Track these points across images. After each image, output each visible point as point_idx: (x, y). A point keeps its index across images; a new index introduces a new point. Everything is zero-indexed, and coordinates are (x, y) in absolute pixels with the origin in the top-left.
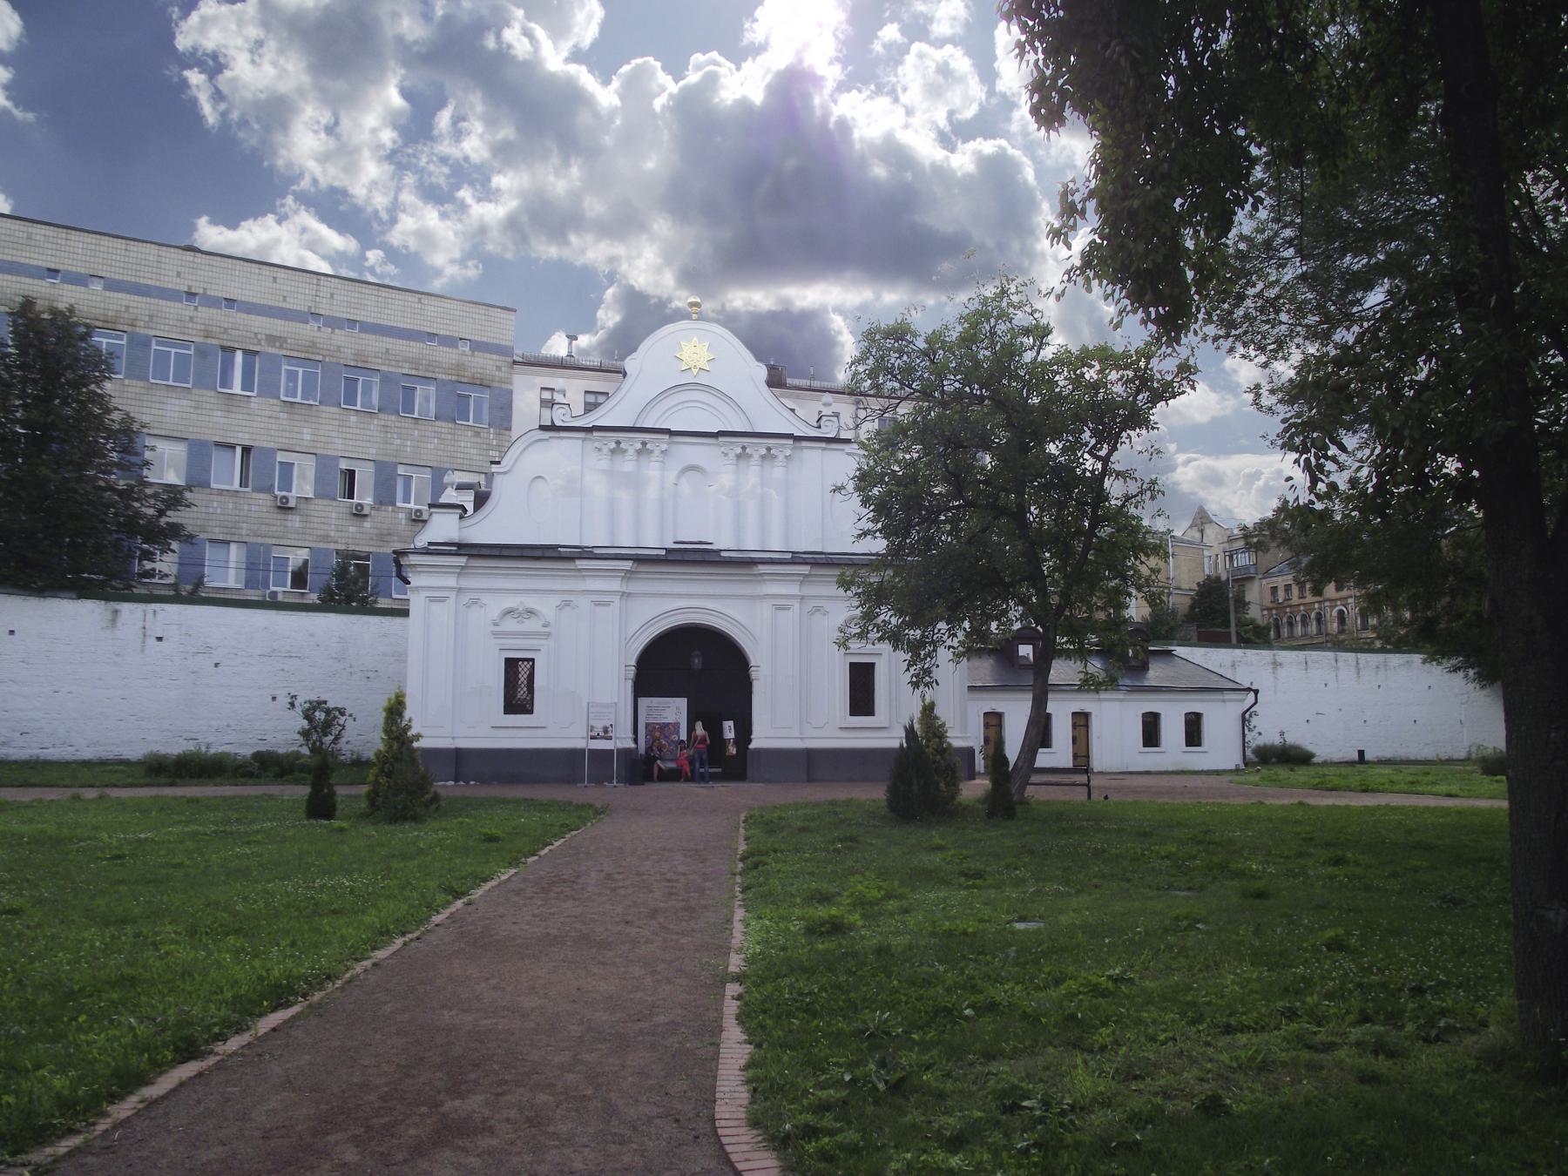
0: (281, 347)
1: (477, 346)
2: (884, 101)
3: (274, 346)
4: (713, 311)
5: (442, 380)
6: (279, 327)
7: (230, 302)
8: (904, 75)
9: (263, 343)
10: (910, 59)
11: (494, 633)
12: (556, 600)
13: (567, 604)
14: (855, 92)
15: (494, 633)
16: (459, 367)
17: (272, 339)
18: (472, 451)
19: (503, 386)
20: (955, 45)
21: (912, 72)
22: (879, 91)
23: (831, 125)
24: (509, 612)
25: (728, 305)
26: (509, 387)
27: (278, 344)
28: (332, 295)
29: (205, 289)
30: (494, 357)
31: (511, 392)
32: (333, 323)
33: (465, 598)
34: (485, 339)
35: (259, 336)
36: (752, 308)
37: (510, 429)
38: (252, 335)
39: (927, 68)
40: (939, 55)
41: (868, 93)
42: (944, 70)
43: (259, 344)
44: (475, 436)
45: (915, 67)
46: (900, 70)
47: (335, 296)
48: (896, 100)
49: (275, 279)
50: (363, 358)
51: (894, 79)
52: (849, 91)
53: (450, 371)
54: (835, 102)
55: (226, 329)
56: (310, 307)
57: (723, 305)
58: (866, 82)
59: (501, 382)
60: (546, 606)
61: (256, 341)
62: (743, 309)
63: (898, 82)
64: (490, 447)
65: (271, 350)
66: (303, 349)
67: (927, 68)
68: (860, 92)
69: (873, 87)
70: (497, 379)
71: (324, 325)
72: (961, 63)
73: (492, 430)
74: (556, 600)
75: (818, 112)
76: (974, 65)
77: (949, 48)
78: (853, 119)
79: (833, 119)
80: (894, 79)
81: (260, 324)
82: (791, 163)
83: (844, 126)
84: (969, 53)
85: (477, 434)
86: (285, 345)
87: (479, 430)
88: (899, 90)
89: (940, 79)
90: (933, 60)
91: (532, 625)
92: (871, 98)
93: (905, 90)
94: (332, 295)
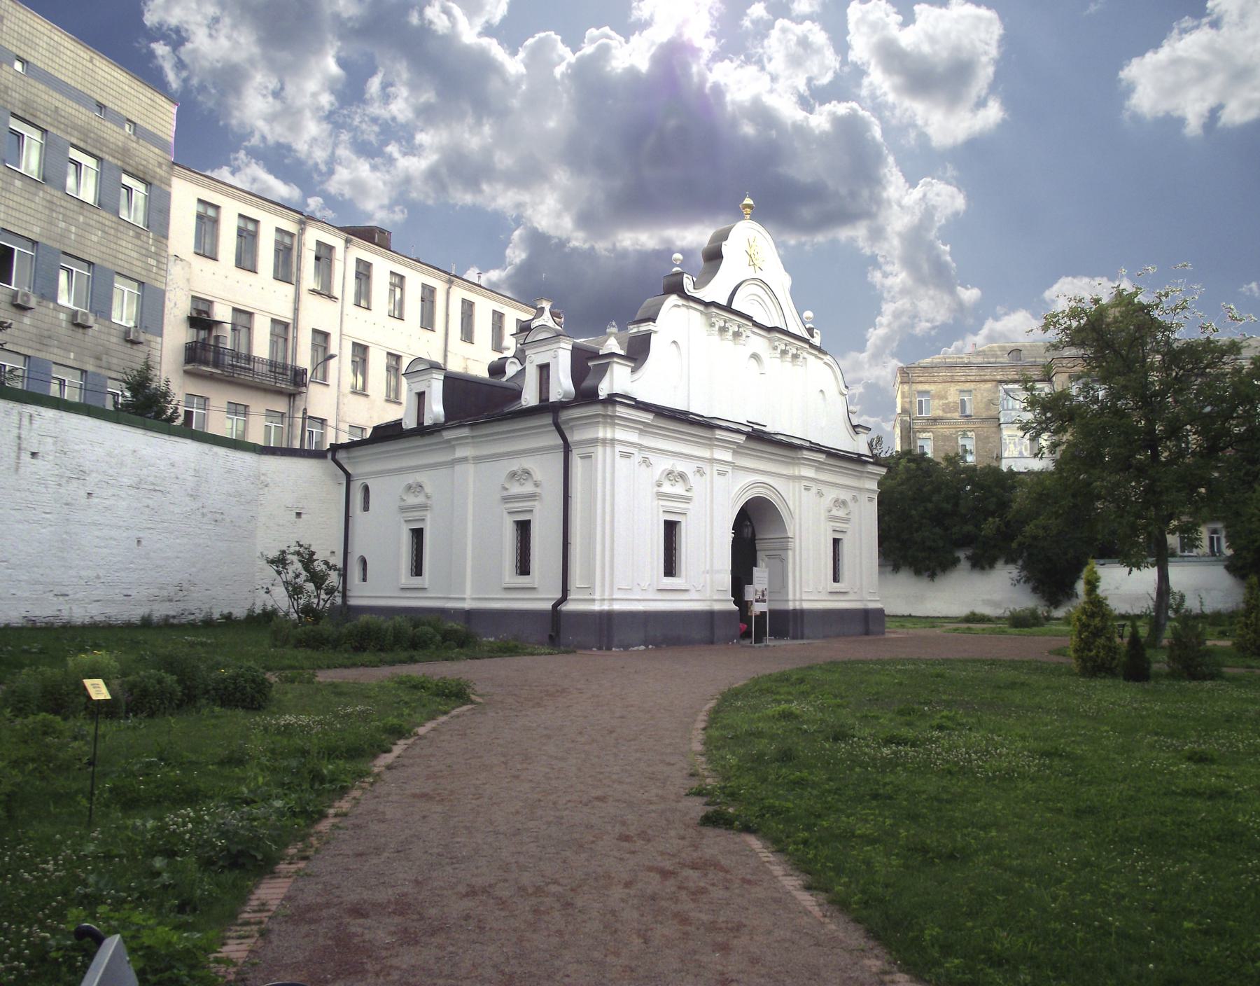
2: (752, 69)
4: (606, 250)
5: (109, 163)
8: (770, 47)
10: (775, 33)
14: (727, 61)
20: (813, 21)
21: (776, 45)
22: (748, 60)
23: (707, 90)
25: (618, 245)
36: (638, 247)
39: (789, 41)
40: (799, 29)
41: (739, 62)
42: (804, 43)
45: (780, 41)
46: (766, 42)
48: (763, 68)
51: (761, 51)
52: (722, 60)
53: (116, 154)
54: (710, 70)
57: (614, 245)
58: (737, 54)
62: (631, 248)
63: (764, 53)
67: (789, 41)
68: (732, 62)
69: (742, 57)
72: (819, 36)
75: (696, 79)
76: (830, 39)
77: (808, 24)
78: (725, 84)
79: (708, 85)
80: (761, 51)
82: (672, 123)
83: (718, 91)
84: (825, 28)
88: (765, 60)
89: (800, 51)
90: (794, 34)
92: (742, 67)
93: (770, 60)
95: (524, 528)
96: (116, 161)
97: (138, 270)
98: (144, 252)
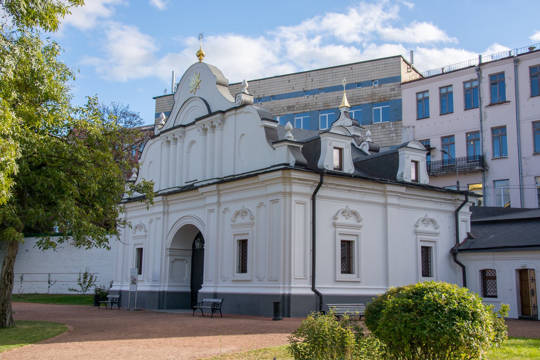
0: (293, 110)
1: (382, 82)
3: (290, 111)
6: (291, 101)
7: (273, 97)
9: (286, 110)
11: (232, 226)
12: (257, 202)
13: (261, 204)
15: (232, 226)
16: (373, 94)
17: (289, 108)
18: (381, 136)
19: (396, 98)
24: (237, 214)
26: (400, 98)
27: (291, 109)
28: (312, 80)
29: (264, 95)
30: (391, 84)
31: (400, 100)
32: (313, 92)
33: (222, 209)
34: (386, 77)
35: (284, 108)
37: (401, 120)
38: (282, 108)
43: (284, 111)
44: (382, 128)
47: (314, 80)
49: (289, 81)
50: (327, 105)
55: (272, 109)
56: (303, 89)
59: (395, 96)
60: (251, 206)
61: (283, 110)
64: (391, 132)
65: (289, 113)
66: (302, 108)
70: (393, 95)
71: (310, 95)
73: (391, 123)
74: (257, 202)
81: (285, 103)
85: (384, 127)
86: (294, 109)
87: (384, 125)
91: (247, 219)
94: (312, 80)
95: (426, 252)
96: (368, 101)
97: (386, 142)
98: (388, 132)
